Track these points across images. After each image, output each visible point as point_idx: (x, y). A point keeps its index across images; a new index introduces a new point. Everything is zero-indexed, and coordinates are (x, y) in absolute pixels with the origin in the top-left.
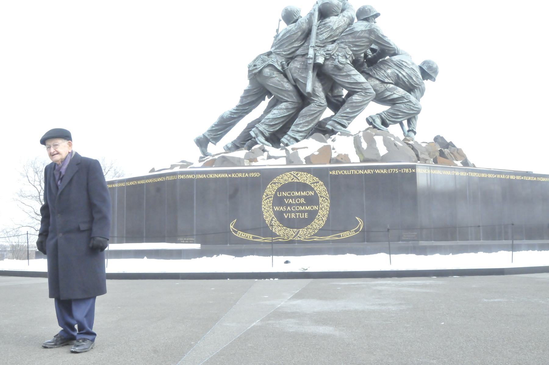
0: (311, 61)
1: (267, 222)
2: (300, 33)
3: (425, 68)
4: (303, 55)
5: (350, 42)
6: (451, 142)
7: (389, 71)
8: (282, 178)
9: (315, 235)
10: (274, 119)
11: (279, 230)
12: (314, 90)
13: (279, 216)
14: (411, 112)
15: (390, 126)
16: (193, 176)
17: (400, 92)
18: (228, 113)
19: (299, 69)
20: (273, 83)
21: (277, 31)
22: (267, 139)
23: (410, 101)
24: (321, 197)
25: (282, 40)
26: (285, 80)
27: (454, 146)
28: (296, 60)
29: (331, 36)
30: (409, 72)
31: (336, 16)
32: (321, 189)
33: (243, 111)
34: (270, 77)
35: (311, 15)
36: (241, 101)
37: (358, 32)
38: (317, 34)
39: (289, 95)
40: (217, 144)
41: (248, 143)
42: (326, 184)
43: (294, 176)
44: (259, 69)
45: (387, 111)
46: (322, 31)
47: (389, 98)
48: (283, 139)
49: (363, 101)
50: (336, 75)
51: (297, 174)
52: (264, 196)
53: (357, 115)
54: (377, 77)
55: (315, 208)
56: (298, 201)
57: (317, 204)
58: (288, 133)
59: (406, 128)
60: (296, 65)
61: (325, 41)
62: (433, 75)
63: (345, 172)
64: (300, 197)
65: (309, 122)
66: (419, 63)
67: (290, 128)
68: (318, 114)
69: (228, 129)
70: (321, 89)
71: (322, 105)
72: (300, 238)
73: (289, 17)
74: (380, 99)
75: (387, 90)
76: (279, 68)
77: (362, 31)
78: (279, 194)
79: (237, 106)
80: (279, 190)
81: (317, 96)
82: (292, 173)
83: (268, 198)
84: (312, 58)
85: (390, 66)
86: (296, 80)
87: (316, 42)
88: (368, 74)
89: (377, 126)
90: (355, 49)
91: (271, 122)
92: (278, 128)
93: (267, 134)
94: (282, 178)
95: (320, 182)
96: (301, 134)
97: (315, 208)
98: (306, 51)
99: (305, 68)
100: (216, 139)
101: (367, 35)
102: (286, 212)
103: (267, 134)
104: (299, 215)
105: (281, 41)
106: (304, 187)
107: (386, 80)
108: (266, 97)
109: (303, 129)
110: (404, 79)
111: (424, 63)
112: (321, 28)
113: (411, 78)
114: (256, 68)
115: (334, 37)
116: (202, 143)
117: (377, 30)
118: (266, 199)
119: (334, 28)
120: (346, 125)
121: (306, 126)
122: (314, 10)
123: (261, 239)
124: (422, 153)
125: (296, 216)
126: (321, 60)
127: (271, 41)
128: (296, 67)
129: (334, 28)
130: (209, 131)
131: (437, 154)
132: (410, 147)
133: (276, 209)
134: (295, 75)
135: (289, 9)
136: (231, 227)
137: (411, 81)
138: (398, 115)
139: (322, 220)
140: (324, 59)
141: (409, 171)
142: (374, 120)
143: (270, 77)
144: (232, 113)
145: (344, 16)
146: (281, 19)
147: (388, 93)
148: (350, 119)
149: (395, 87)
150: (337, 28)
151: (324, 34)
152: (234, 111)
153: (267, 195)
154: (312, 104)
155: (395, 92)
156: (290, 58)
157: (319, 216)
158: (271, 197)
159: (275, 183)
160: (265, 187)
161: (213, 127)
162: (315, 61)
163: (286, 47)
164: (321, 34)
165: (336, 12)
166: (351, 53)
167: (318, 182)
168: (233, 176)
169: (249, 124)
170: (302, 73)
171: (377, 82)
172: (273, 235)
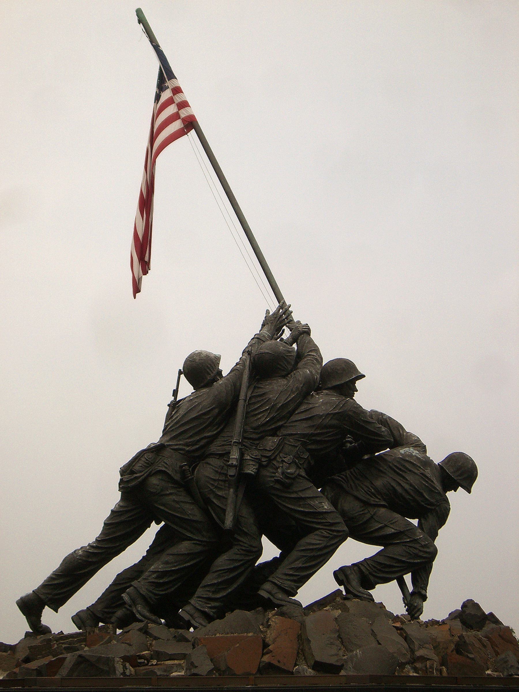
0: (232, 472)
2: (216, 411)
4: (221, 456)
5: (304, 436)
7: (379, 483)
10: (164, 574)
12: (237, 520)
15: (377, 586)
19: (215, 480)
21: (175, 393)
23: (415, 541)
26: (188, 499)
27: (497, 621)
38: (247, 415)
40: (60, 609)
41: (120, 613)
46: (256, 409)
49: (326, 547)
54: (356, 493)
58: (192, 601)
60: (206, 472)
61: (262, 429)
67: (193, 594)
70: (251, 521)
73: (200, 370)
76: (177, 477)
84: (235, 466)
86: (208, 501)
90: (313, 447)
92: (173, 589)
98: (227, 448)
100: (56, 604)
101: (334, 422)
107: (373, 500)
109: (219, 596)
110: (408, 497)
112: (254, 403)
115: (278, 421)
116: (31, 607)
117: (354, 412)
124: (421, 647)
126: (251, 469)
132: (401, 635)
142: (346, 576)
148: (303, 580)
154: (235, 549)
161: (50, 579)
166: (306, 455)
169: (118, 575)
171: (357, 504)
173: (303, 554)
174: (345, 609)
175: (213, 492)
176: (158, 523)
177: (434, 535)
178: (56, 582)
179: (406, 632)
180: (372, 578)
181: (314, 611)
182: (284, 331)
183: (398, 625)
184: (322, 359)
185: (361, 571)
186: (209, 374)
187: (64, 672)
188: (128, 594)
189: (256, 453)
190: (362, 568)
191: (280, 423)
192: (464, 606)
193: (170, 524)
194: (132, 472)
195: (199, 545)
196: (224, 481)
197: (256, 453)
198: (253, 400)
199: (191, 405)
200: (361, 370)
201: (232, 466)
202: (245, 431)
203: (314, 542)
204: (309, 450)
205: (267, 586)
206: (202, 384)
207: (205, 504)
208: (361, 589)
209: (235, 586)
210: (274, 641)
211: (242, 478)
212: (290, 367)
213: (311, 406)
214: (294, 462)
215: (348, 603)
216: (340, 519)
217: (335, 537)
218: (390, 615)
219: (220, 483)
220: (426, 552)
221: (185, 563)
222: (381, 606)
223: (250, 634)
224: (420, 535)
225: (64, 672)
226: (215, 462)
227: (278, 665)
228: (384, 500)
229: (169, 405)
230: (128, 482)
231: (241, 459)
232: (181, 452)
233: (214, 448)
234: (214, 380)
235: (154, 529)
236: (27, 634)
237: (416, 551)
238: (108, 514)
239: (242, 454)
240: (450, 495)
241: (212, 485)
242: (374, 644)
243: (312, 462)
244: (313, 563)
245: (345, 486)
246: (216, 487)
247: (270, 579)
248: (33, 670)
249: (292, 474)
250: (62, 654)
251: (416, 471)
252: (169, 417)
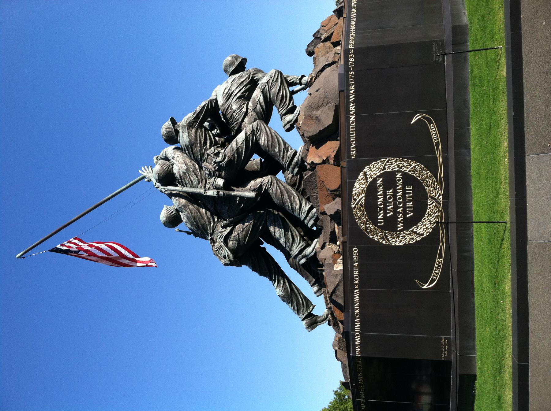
0: (221, 193)
1: (418, 239)
6: (314, 36)
7: (234, 107)
8: (360, 219)
9: (436, 176)
11: (424, 227)
12: (253, 190)
13: (409, 223)
14: (279, 80)
15: (295, 104)
16: (358, 335)
17: (257, 94)
21: (188, 233)
22: (310, 245)
24: (384, 169)
29: (194, 172)
30: (235, 85)
31: (173, 167)
32: (373, 170)
34: (239, 240)
36: (265, 275)
37: (190, 140)
42: (368, 163)
43: (357, 204)
44: (229, 252)
47: (264, 107)
48: (309, 225)
51: (355, 200)
52: (384, 242)
53: (283, 140)
54: (240, 120)
55: (399, 175)
56: (390, 198)
57: (394, 173)
62: (239, 60)
63: (352, 139)
64: (384, 195)
68: (280, 185)
69: (296, 290)
71: (270, 180)
72: (440, 195)
74: (265, 115)
75: (254, 109)
76: (229, 229)
77: (189, 136)
78: (381, 222)
79: (271, 280)
80: (375, 221)
81: (261, 186)
82: (353, 206)
83: (386, 237)
84: (218, 192)
85: (229, 106)
87: (201, 187)
89: (295, 118)
90: (208, 144)
91: (289, 239)
93: (302, 244)
94: (360, 219)
95: (365, 170)
96: (303, 204)
97: (399, 175)
102: (404, 213)
103: (302, 244)
104: (409, 197)
106: (371, 190)
107: (244, 110)
109: (298, 202)
110: (243, 90)
112: (186, 183)
116: (313, 322)
118: (388, 240)
119: (185, 167)
120: (293, 151)
121: (294, 199)
123: (442, 247)
125: (409, 201)
126: (220, 182)
129: (185, 167)
130: (298, 313)
131: (328, 44)
132: (319, 76)
133: (400, 226)
136: (425, 286)
137: (245, 83)
139: (415, 167)
140: (219, 179)
142: (288, 122)
146: (176, 229)
147: (258, 106)
149: (251, 100)
150: (186, 164)
151: (192, 179)
153: (382, 238)
155: (257, 100)
157: (410, 171)
158: (385, 233)
159: (367, 228)
160: (373, 240)
162: (220, 189)
164: (192, 182)
166: (213, 149)
167: (365, 173)
168: (357, 282)
171: (246, 120)
172: (435, 231)
178: (296, 307)
203: (263, 139)
210: (319, 157)
227: (335, 152)
229: (196, 237)
235: (265, 245)
236: (329, 324)
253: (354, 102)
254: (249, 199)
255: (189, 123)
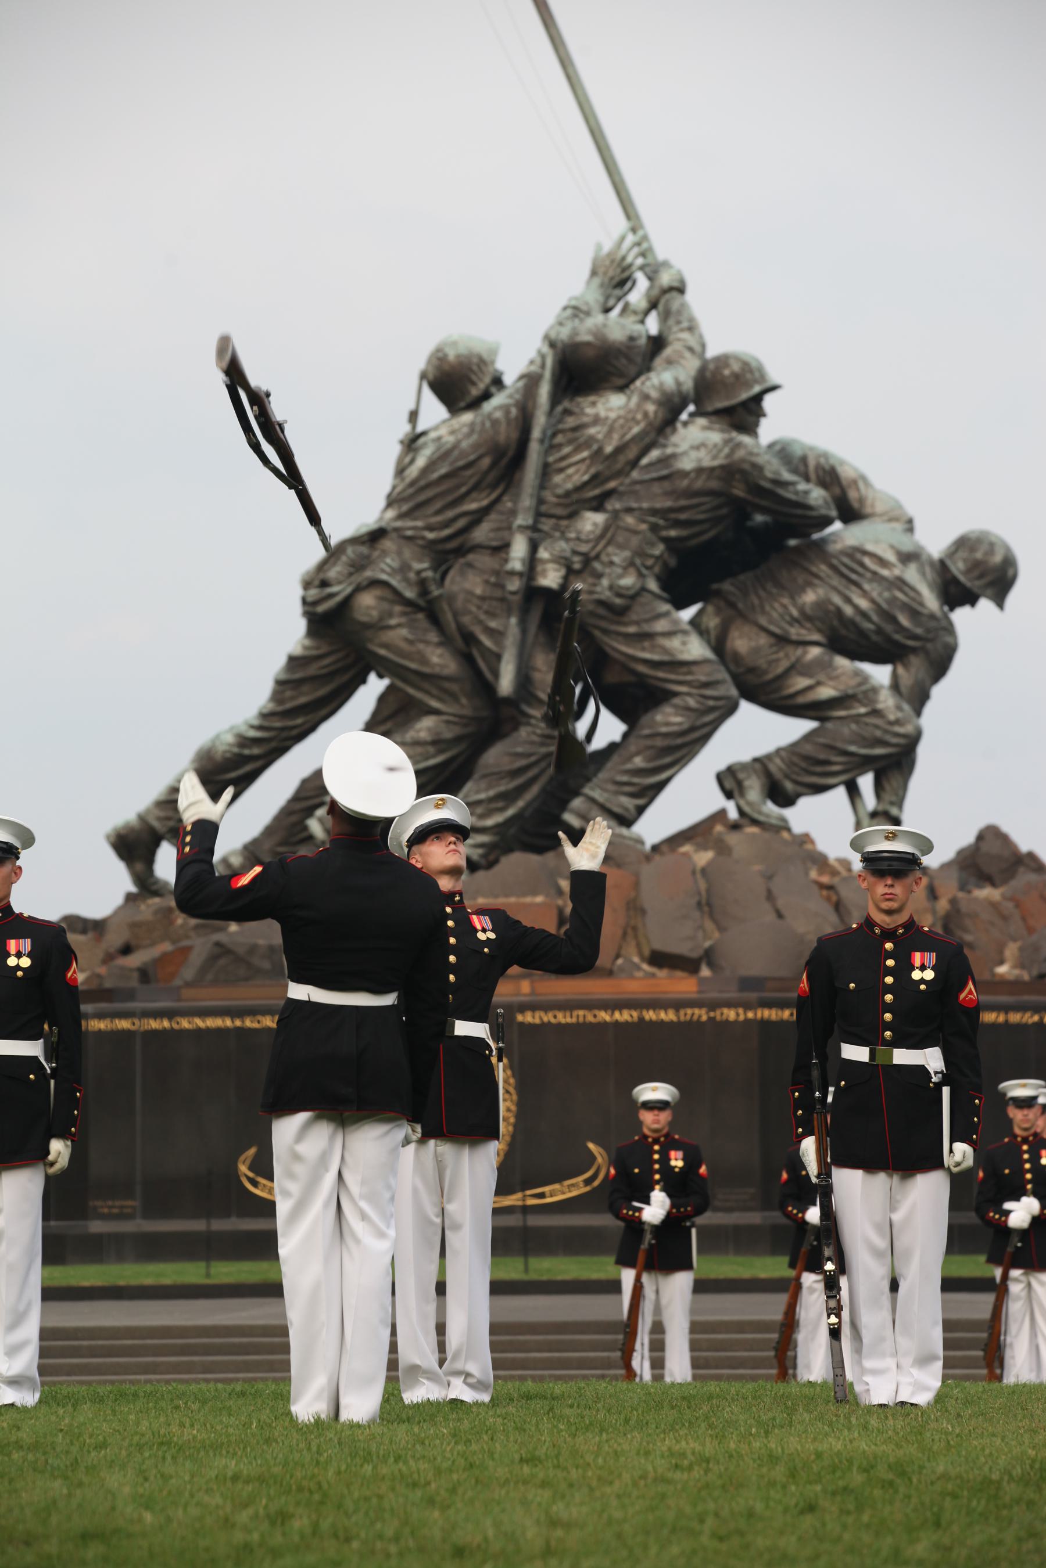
0: (514, 585)
2: (486, 462)
3: (958, 568)
5: (654, 512)
7: (810, 597)
18: (230, 738)
19: (482, 598)
20: (386, 646)
21: (413, 416)
23: (876, 713)
25: (428, 486)
26: (433, 637)
28: (470, 565)
29: (594, 477)
33: (285, 734)
35: (531, 381)
36: (277, 696)
38: (546, 471)
39: (445, 691)
44: (338, 599)
45: (793, 749)
47: (801, 700)
49: (692, 729)
50: (605, 632)
54: (763, 621)
59: (869, 799)
60: (467, 583)
61: (575, 497)
65: (508, 797)
66: (935, 541)
76: (410, 594)
77: (700, 471)
79: (264, 716)
84: (520, 574)
86: (469, 638)
88: (732, 605)
90: (673, 533)
99: (497, 600)
101: (714, 484)
105: (419, 485)
107: (794, 632)
108: (372, 677)
109: (490, 822)
111: (963, 543)
112: (560, 446)
113: (894, 620)
114: (331, 596)
115: (608, 479)
122: (543, 366)
126: (551, 578)
127: (384, 482)
128: (471, 593)
129: (609, 449)
132: (828, 899)
134: (466, 620)
135: (451, 355)
136: (243, 1169)
137: (889, 628)
138: (828, 763)
140: (563, 572)
141: (738, 1015)
142: (739, 784)
143: (379, 626)
144: (244, 741)
145: (646, 397)
147: (801, 682)
150: (619, 450)
151: (570, 471)
152: (253, 734)
154: (523, 732)
156: (447, 554)
163: (438, 512)
164: (561, 470)
165: (621, 374)
166: (659, 549)
170: (491, 614)
171: (763, 640)
173: (649, 742)
174: (722, 849)
175: (480, 622)
176: (381, 676)
177: (919, 699)
179: (837, 893)
180: (789, 786)
181: (662, 854)
182: (634, 283)
183: (825, 879)
184: (703, 346)
185: (768, 774)
186: (474, 384)
187: (188, 973)
188: (321, 821)
189: (562, 546)
190: (773, 768)
191: (612, 484)
192: (980, 837)
193: (400, 684)
194: (324, 584)
195: (454, 723)
196: (502, 600)
197: (562, 546)
198: (559, 439)
199: (438, 449)
200: (774, 376)
201: (512, 573)
202: (541, 501)
204: (666, 540)
205: (577, 803)
206: (462, 404)
207: (466, 647)
208: (770, 807)
209: (520, 804)
211: (533, 593)
212: (632, 370)
213: (669, 451)
214: (631, 564)
215: (733, 839)
216: (723, 675)
217: (712, 709)
218: (820, 861)
219: (494, 603)
220: (897, 735)
221: (427, 759)
222: (805, 839)
223: (539, 899)
224: (887, 701)
225: (188, 973)
226: (484, 560)
228: (819, 631)
229: (402, 442)
230: (315, 603)
231: (532, 561)
232: (421, 542)
233: (481, 534)
234: (486, 396)
236: (130, 898)
237: (878, 733)
238: (281, 661)
239: (534, 547)
240: (961, 617)
241: (479, 608)
242: (770, 917)
243: (673, 562)
244: (667, 760)
245: (740, 605)
246: (487, 612)
247: (587, 790)
248: (131, 970)
249: (628, 588)
250: (188, 937)
251: (885, 572)
252: (400, 471)
253: (641, 1019)
254: (496, 674)
255: (743, 472)
